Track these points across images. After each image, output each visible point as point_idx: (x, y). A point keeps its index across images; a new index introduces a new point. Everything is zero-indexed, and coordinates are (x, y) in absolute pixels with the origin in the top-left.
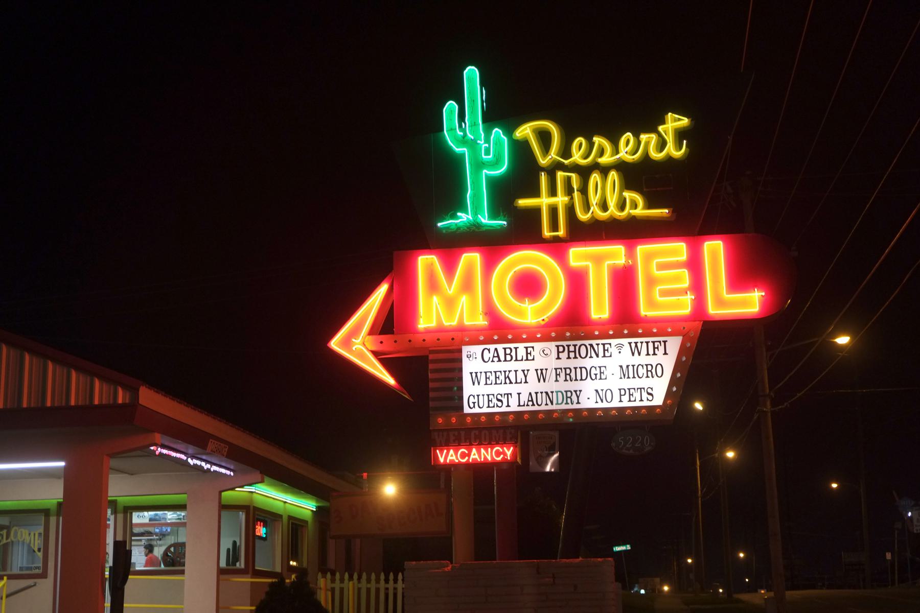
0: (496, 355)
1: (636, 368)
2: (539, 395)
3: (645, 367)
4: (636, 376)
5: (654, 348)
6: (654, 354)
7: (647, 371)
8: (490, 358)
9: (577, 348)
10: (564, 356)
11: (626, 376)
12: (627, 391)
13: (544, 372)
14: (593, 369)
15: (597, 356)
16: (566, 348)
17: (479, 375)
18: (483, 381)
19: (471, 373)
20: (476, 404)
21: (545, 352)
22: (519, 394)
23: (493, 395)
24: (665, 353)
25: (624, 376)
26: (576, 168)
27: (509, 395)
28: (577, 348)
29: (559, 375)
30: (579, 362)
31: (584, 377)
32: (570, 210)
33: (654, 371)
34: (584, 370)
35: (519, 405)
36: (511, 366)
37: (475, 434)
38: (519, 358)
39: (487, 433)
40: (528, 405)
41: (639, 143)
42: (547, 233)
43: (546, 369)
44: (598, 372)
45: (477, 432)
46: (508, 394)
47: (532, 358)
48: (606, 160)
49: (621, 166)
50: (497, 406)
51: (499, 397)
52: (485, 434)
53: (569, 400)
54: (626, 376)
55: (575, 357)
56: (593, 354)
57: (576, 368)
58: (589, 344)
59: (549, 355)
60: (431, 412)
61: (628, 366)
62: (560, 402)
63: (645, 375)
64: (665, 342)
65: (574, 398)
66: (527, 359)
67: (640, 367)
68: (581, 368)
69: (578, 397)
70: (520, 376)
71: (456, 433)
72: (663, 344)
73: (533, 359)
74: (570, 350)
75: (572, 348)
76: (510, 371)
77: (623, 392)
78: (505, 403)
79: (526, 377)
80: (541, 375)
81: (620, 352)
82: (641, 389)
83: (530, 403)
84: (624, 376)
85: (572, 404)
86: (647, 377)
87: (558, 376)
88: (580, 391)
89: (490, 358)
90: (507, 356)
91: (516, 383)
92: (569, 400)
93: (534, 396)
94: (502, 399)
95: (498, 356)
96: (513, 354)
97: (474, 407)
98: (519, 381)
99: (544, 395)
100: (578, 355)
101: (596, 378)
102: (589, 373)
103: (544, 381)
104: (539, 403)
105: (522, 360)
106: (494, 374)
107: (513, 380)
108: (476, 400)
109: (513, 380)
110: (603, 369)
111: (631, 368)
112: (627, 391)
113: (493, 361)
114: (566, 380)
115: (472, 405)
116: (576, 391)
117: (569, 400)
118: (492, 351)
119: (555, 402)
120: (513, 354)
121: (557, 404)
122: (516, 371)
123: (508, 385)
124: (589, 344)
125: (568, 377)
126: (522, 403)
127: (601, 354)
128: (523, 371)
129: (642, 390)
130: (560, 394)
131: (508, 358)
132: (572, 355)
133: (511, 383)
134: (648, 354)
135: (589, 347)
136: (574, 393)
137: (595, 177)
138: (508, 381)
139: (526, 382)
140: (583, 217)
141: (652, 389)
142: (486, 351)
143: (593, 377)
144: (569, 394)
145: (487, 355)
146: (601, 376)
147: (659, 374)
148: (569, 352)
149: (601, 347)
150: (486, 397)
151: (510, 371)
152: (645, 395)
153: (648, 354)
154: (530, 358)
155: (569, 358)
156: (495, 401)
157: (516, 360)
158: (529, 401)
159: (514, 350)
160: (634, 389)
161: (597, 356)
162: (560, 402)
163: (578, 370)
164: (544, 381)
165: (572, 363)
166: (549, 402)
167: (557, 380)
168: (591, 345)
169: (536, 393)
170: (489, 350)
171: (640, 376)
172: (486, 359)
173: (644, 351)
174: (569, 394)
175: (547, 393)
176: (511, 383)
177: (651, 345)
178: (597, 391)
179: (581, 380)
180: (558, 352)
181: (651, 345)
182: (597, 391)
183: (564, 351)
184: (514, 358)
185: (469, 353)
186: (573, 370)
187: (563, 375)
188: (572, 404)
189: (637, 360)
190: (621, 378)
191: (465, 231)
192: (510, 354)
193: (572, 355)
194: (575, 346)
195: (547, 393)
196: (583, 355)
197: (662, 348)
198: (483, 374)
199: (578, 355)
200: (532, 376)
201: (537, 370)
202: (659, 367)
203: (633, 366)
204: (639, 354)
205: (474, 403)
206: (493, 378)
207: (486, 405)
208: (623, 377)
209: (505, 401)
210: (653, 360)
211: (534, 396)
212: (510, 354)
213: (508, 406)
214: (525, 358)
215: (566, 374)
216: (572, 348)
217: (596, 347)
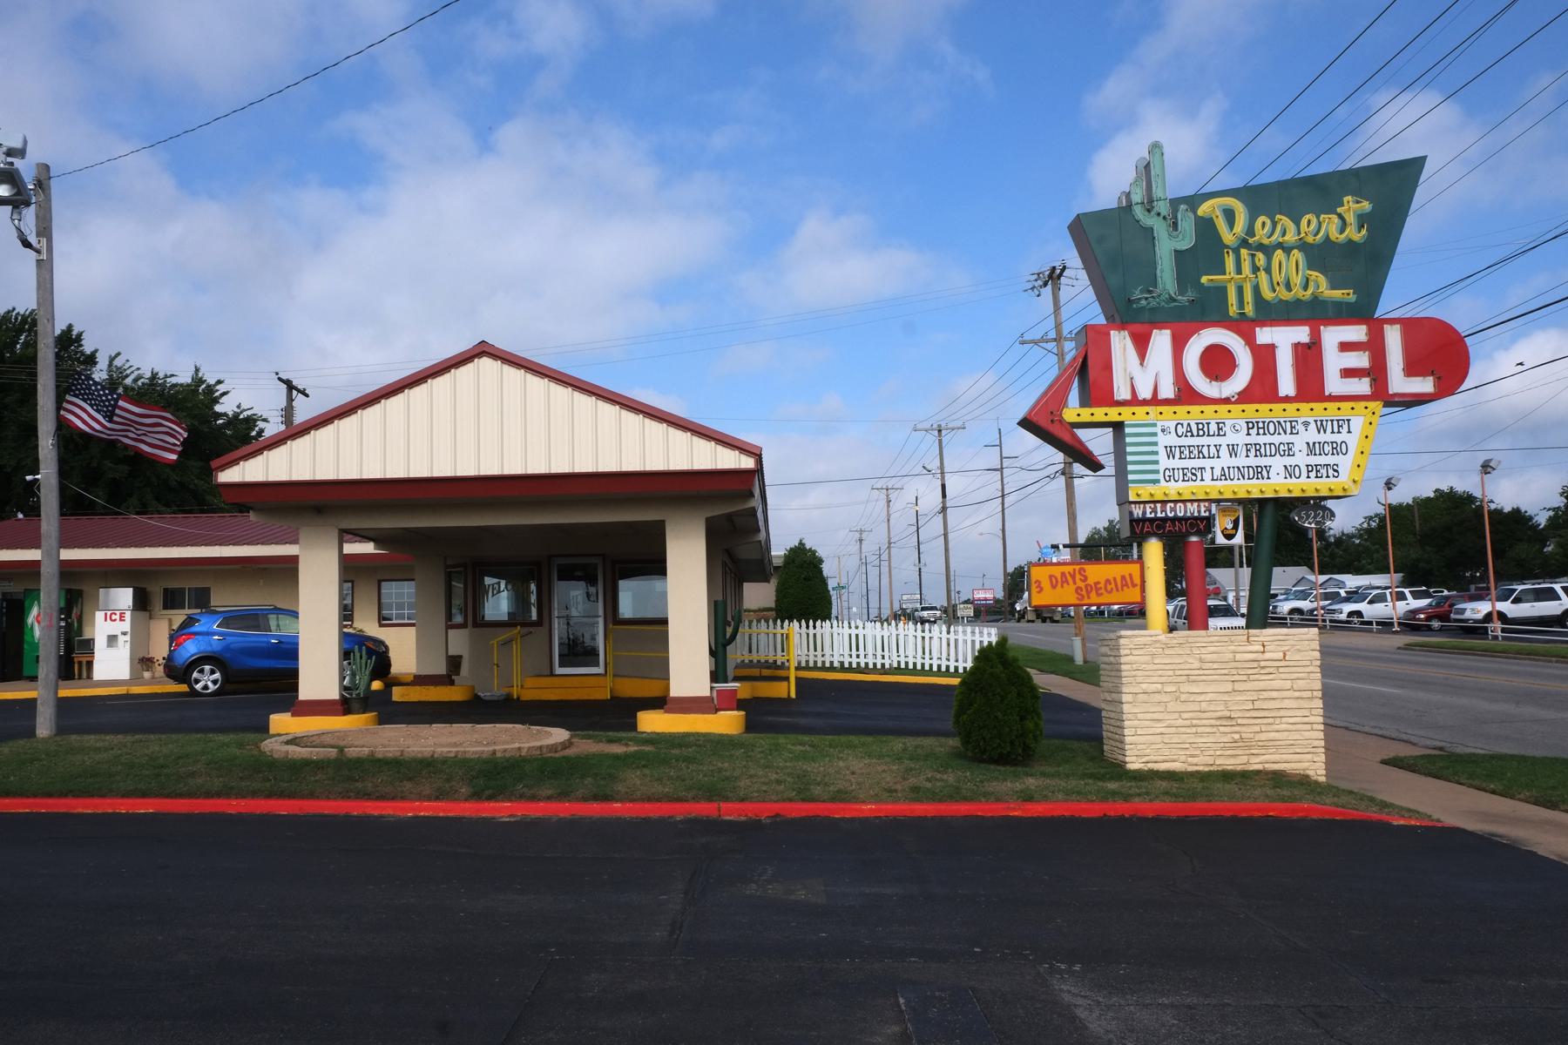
1: (1322, 444)
2: (1231, 470)
5: (1339, 426)
6: (1339, 432)
7: (1333, 448)
13: (1235, 447)
15: (1285, 433)
17: (1173, 449)
18: (1177, 455)
19: (1166, 447)
22: (1212, 468)
23: (1187, 469)
24: (1349, 432)
26: (1261, 247)
30: (1268, 439)
32: (1257, 290)
33: (1338, 448)
35: (1213, 480)
38: (1211, 433)
39: (1182, 505)
40: (1221, 480)
42: (1233, 310)
43: (1238, 445)
44: (1286, 448)
45: (1172, 505)
46: (1201, 469)
48: (1291, 237)
49: (1303, 246)
51: (1193, 471)
55: (1264, 434)
56: (1281, 431)
60: (1130, 485)
61: (1314, 443)
62: (1251, 477)
63: (1331, 452)
64: (1349, 420)
65: (1265, 473)
66: (1219, 435)
67: (1326, 444)
68: (1270, 444)
69: (1268, 472)
70: (1213, 450)
71: (1152, 506)
72: (1346, 422)
73: (1225, 435)
75: (1261, 425)
76: (1203, 446)
77: (1310, 468)
78: (1199, 478)
79: (1218, 451)
80: (1233, 451)
82: (1327, 465)
86: (1333, 454)
88: (1270, 467)
93: (1226, 470)
95: (1191, 431)
96: (1206, 429)
97: (1170, 480)
98: (1211, 456)
99: (1236, 469)
100: (1266, 432)
102: (1277, 450)
105: (1214, 435)
106: (1187, 448)
107: (1207, 456)
108: (1171, 474)
109: (1207, 456)
111: (1317, 445)
113: (1186, 436)
114: (1256, 456)
115: (1167, 479)
116: (1266, 467)
117: (1260, 475)
118: (1185, 425)
119: (1246, 477)
120: (1206, 429)
121: (1249, 479)
122: (1209, 446)
127: (1289, 431)
128: (1215, 446)
131: (1201, 433)
132: (1261, 431)
133: (1204, 457)
134: (1333, 432)
135: (1277, 424)
139: (1218, 457)
140: (1268, 294)
141: (1337, 465)
142: (1179, 426)
143: (1282, 453)
144: (1260, 470)
145: (1180, 432)
146: (1289, 452)
148: (1258, 428)
149: (1288, 424)
150: (1181, 471)
151: (1203, 446)
153: (1333, 432)
154: (1221, 433)
155: (1258, 434)
156: (1189, 474)
157: (1208, 435)
159: (1206, 426)
161: (1285, 433)
162: (1251, 477)
163: (1268, 446)
165: (1262, 439)
167: (1247, 456)
168: (1279, 422)
169: (1229, 468)
170: (1182, 425)
172: (1180, 434)
173: (1329, 429)
174: (1260, 470)
175: (1238, 468)
176: (1204, 457)
177: (1335, 423)
178: (1285, 466)
180: (1248, 429)
181: (1335, 423)
182: (1285, 466)
187: (1253, 450)
189: (1322, 437)
190: (1308, 455)
192: (1202, 429)
193: (1261, 431)
195: (1238, 468)
196: (1272, 431)
197: (1345, 427)
198: (1178, 449)
199: (1266, 432)
200: (1224, 452)
201: (1228, 445)
203: (1320, 443)
205: (1170, 476)
206: (1187, 452)
207: (1181, 478)
210: (1338, 438)
211: (1226, 470)
212: (1202, 429)
213: (1202, 480)
214: (1216, 433)
215: (1256, 450)
216: (1261, 425)
217: (1283, 424)
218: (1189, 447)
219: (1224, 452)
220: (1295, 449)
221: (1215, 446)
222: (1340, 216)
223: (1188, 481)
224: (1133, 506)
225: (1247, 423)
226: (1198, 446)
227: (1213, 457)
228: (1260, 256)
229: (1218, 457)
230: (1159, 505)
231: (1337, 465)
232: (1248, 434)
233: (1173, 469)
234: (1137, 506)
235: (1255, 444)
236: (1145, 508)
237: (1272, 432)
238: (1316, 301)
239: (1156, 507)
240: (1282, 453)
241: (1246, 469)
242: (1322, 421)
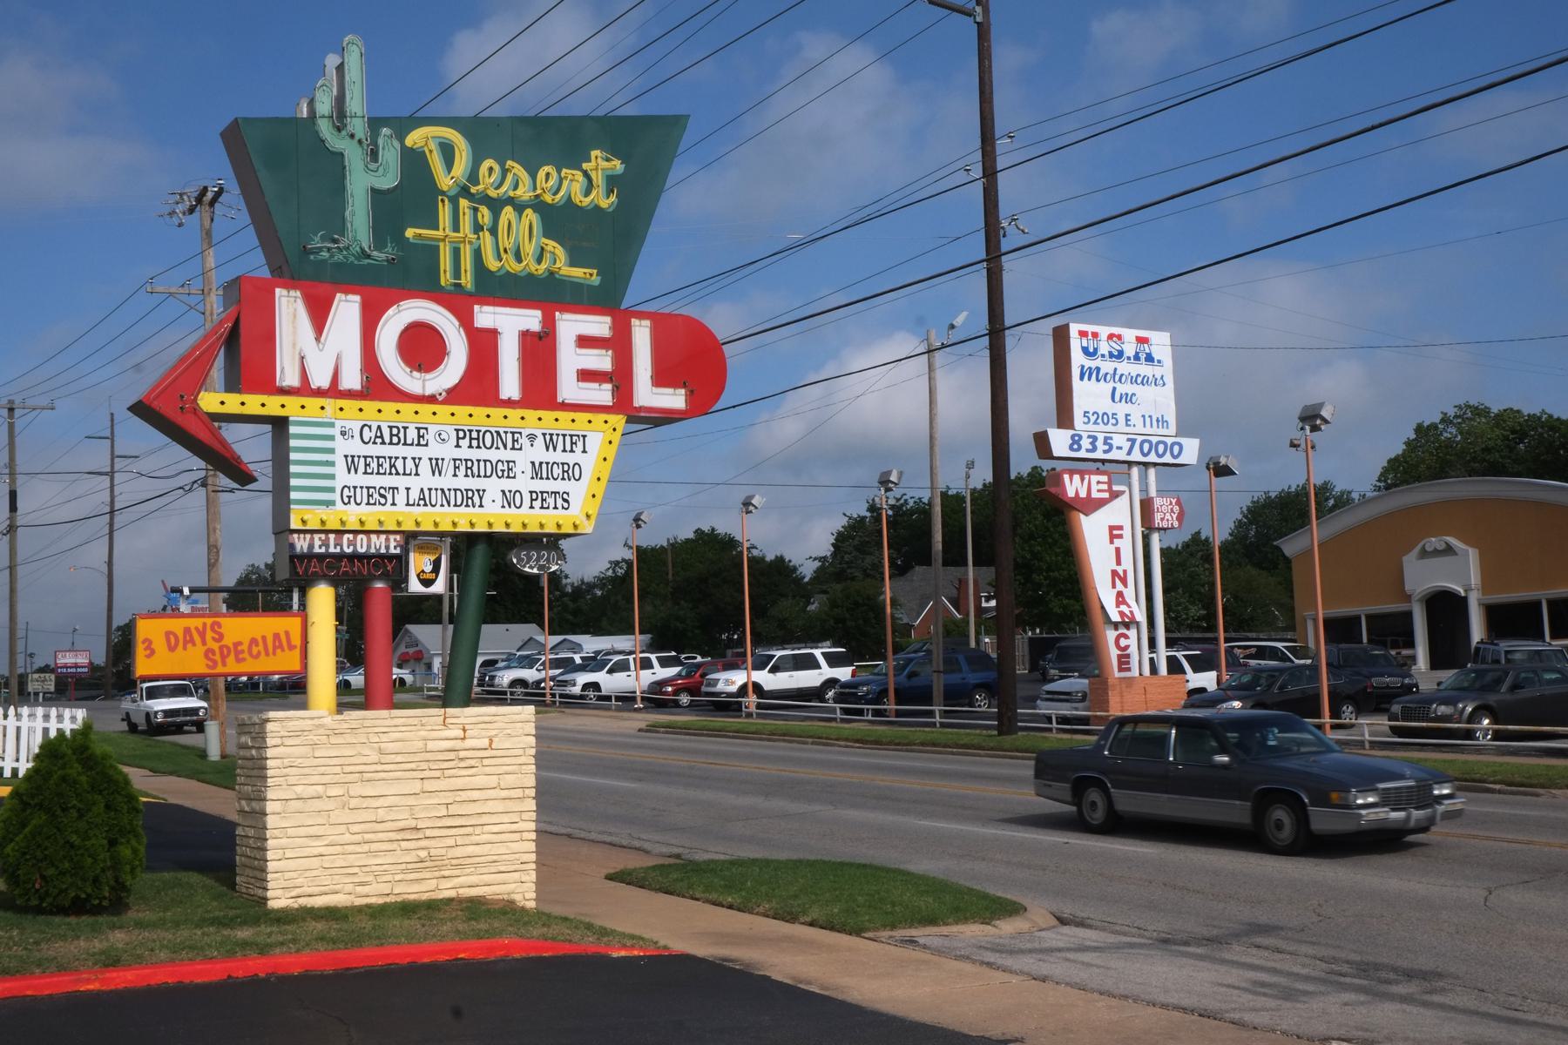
0: (379, 434)
1: (551, 465)
2: (433, 492)
3: (561, 466)
4: (550, 476)
5: (572, 443)
6: (572, 451)
7: (564, 471)
8: (371, 438)
9: (481, 434)
10: (465, 443)
11: (539, 476)
12: (540, 495)
13: (440, 462)
14: (500, 463)
16: (468, 433)
17: (356, 459)
19: (346, 456)
20: (352, 499)
21: (442, 437)
22: (408, 489)
23: (375, 488)
24: (584, 451)
25: (537, 475)
27: (396, 491)
28: (481, 434)
29: (458, 467)
30: (483, 454)
31: (488, 474)
32: (478, 255)
33: (570, 472)
34: (488, 464)
35: (408, 504)
36: (399, 451)
38: (409, 442)
40: (419, 505)
42: (446, 279)
43: (443, 459)
44: (506, 468)
45: (351, 536)
46: (393, 489)
47: (425, 443)
48: (524, 193)
49: (538, 205)
50: (380, 503)
51: (382, 491)
54: (539, 476)
55: (479, 447)
56: (500, 445)
57: (479, 461)
60: (292, 506)
61: (541, 463)
62: (459, 503)
63: (561, 476)
64: (584, 436)
65: (476, 499)
66: (419, 444)
67: (555, 466)
68: (485, 461)
69: (481, 498)
70: (410, 464)
71: (323, 536)
72: (581, 439)
73: (426, 445)
75: (474, 435)
76: (397, 458)
77: (534, 496)
78: (390, 501)
79: (417, 466)
80: (436, 466)
81: (532, 445)
82: (555, 493)
83: (422, 502)
84: (537, 475)
85: (474, 506)
86: (563, 479)
88: (484, 491)
89: (371, 438)
90: (476, 437)
91: (404, 474)
93: (427, 493)
94: (387, 494)
95: (382, 437)
96: (401, 435)
97: (349, 502)
98: (408, 472)
99: (440, 492)
100: (481, 445)
101: (503, 476)
102: (494, 469)
104: (433, 503)
105: (412, 444)
106: (375, 460)
107: (401, 471)
108: (352, 494)
109: (401, 471)
110: (511, 464)
111: (544, 466)
112: (540, 495)
113: (375, 443)
114: (466, 476)
115: (346, 500)
116: (478, 491)
117: (470, 501)
118: (374, 428)
119: (452, 503)
120: (401, 435)
121: (455, 505)
122: (404, 458)
126: (411, 502)
127: (509, 445)
128: (414, 459)
130: (459, 493)
132: (475, 443)
133: (397, 474)
134: (564, 451)
135: (495, 435)
136: (476, 493)
137: (508, 213)
138: (393, 471)
139: (417, 474)
140: (492, 264)
141: (568, 494)
142: (366, 429)
143: (500, 474)
144: (470, 494)
145: (367, 434)
146: (509, 472)
148: (471, 439)
149: (509, 436)
150: (365, 490)
151: (397, 458)
152: (560, 502)
153: (564, 451)
154: (422, 442)
155: (470, 446)
156: (376, 496)
157: (405, 444)
158: (420, 499)
159: (402, 430)
160: (548, 493)
162: (459, 503)
163: (482, 464)
165: (475, 454)
166: (445, 503)
167: (455, 475)
168: (498, 433)
169: (430, 490)
170: (370, 427)
171: (555, 476)
172: (366, 440)
173: (560, 447)
174: (470, 494)
175: (442, 490)
176: (397, 474)
177: (568, 438)
178: (503, 492)
179: (485, 476)
180: (458, 438)
181: (568, 438)
182: (503, 492)
183: (464, 438)
184: (402, 441)
185: (343, 429)
186: (476, 463)
187: (463, 468)
189: (551, 456)
190: (532, 478)
192: (397, 435)
193: (475, 443)
194: (478, 431)
195: (442, 490)
196: (488, 444)
197: (580, 444)
198: (362, 460)
199: (481, 445)
200: (425, 467)
201: (430, 459)
202: (577, 467)
203: (547, 463)
204: (555, 449)
205: (349, 497)
206: (374, 465)
207: (365, 501)
208: (534, 476)
210: (570, 458)
211: (427, 493)
212: (397, 435)
213: (394, 504)
214: (416, 442)
215: (467, 468)
216: (474, 435)
217: (503, 435)
218: (378, 458)
219: (425, 467)
220: (517, 470)
221: (414, 459)
222: (586, 174)
223: (375, 504)
224: (295, 536)
225: (457, 430)
226: (390, 458)
227: (410, 474)
228: (484, 210)
229: (417, 474)
230: (332, 536)
231: (568, 494)
232: (458, 446)
233: (355, 488)
234: (302, 536)
235: (466, 460)
236: (312, 539)
237: (488, 445)
239: (328, 539)
240: (500, 474)
241: (452, 493)
242: (551, 435)
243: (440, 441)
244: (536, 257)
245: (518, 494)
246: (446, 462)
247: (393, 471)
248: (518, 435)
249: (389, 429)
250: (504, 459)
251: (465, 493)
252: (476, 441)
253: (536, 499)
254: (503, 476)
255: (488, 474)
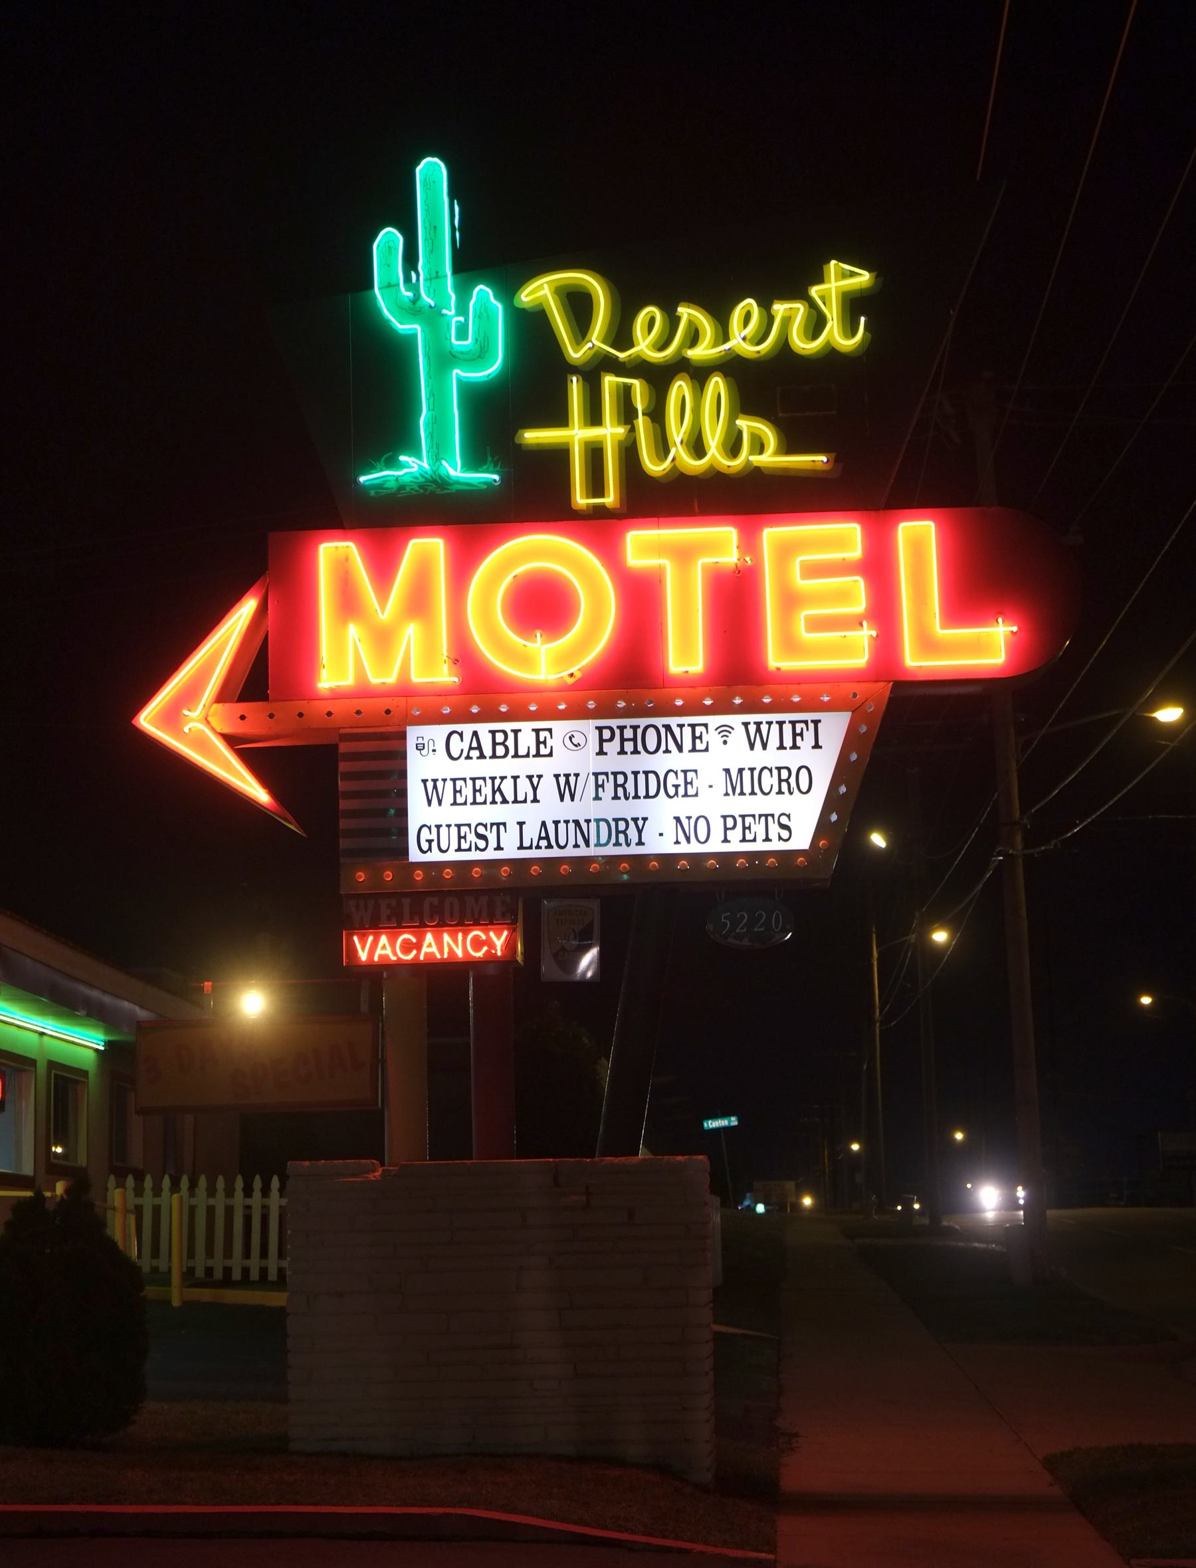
0: (475, 744)
1: (757, 774)
2: (562, 826)
3: (775, 772)
5: (795, 735)
6: (795, 746)
7: (780, 781)
8: (462, 751)
9: (640, 732)
10: (612, 747)
11: (738, 790)
12: (739, 820)
13: (572, 779)
14: (671, 775)
15: (680, 748)
16: (617, 732)
17: (440, 784)
18: (448, 797)
19: (425, 781)
20: (434, 844)
21: (575, 741)
22: (521, 824)
23: (469, 825)
24: (817, 746)
25: (734, 789)
26: (641, 369)
27: (502, 827)
28: (640, 732)
29: (602, 786)
30: (643, 762)
31: (652, 792)
32: (629, 452)
33: (793, 781)
34: (652, 777)
35: (521, 847)
36: (507, 767)
37: (431, 904)
38: (522, 752)
40: (538, 847)
41: (770, 320)
42: (581, 500)
43: (577, 775)
44: (681, 781)
45: (435, 901)
46: (498, 825)
47: (547, 752)
48: (702, 352)
49: (732, 367)
50: (477, 848)
51: (481, 830)
52: (452, 904)
53: (622, 837)
54: (738, 790)
55: (636, 752)
57: (636, 773)
58: (663, 726)
59: (582, 744)
60: (342, 860)
61: (741, 771)
63: (776, 789)
65: (632, 833)
66: (538, 755)
67: (766, 772)
68: (646, 773)
69: (640, 832)
70: (524, 787)
71: (393, 903)
72: (811, 726)
74: (626, 736)
75: (628, 733)
76: (503, 778)
77: (730, 822)
78: (493, 843)
79: (535, 789)
80: (566, 787)
81: (725, 742)
82: (766, 816)
83: (544, 843)
84: (734, 789)
85: (628, 845)
86: (780, 792)
87: (600, 789)
88: (645, 819)
89: (462, 751)
90: (497, 747)
91: (516, 801)
92: (622, 837)
94: (487, 834)
95: (479, 748)
96: (510, 743)
97: (430, 849)
98: (521, 797)
99: (572, 826)
100: (640, 748)
101: (676, 794)
102: (662, 784)
103: (572, 798)
104: (562, 843)
105: (527, 755)
106: (470, 783)
107: (510, 797)
108: (434, 836)
109: (510, 797)
110: (690, 775)
112: (739, 820)
113: (468, 757)
114: (616, 797)
115: (425, 846)
116: (635, 820)
117: (621, 837)
118: (467, 736)
119: (593, 841)
120: (510, 743)
121: (598, 844)
122: (515, 778)
123: (499, 807)
124: (663, 726)
125: (620, 791)
126: (526, 843)
127: (687, 745)
128: (530, 777)
129: (770, 818)
130: (603, 825)
131: (500, 750)
132: (629, 746)
133: (505, 801)
134: (781, 747)
135: (663, 731)
136: (632, 824)
137: (680, 388)
138: (498, 798)
139: (535, 800)
140: (654, 467)
141: (789, 816)
142: (455, 737)
143: (672, 791)
144: (622, 826)
145: (456, 746)
146: (687, 789)
147: (804, 787)
148: (623, 740)
149: (687, 731)
150: (454, 830)
151: (503, 778)
152: (774, 830)
153: (781, 747)
154: (543, 751)
155: (622, 752)
156: (471, 837)
157: (516, 755)
158: (540, 838)
159: (511, 736)
160: (754, 816)
161: (680, 748)
163: (641, 777)
164: (572, 798)
165: (629, 763)
166: (581, 841)
167: (597, 798)
168: (668, 728)
169: (556, 823)
170: (461, 735)
171: (766, 790)
172: (455, 754)
174: (622, 826)
175: (577, 823)
176: (505, 801)
177: (787, 728)
178: (678, 819)
179: (647, 796)
182: (678, 819)
184: (512, 752)
185: (420, 741)
186: (631, 778)
187: (610, 787)
188: (628, 845)
189: (759, 758)
190: (727, 794)
191: (415, 493)
192: (503, 744)
193: (629, 746)
194: (635, 728)
195: (577, 823)
196: (652, 746)
197: (809, 736)
198: (449, 784)
199: (640, 748)
200: (548, 789)
201: (557, 776)
202: (804, 772)
203: (752, 770)
204: (764, 746)
205: (430, 842)
206: (468, 791)
207: (454, 845)
208: (730, 791)
209: (492, 838)
210: (791, 759)
212: (503, 744)
213: (499, 848)
214: (533, 751)
215: (616, 786)
216: (628, 733)
217: (677, 731)
218: (474, 780)
219: (548, 789)
220: (699, 783)
221: (530, 777)
222: (812, 304)
223: (469, 849)
226: (493, 779)
227: (525, 801)
228: (637, 386)
229: (535, 800)
231: (789, 816)
233: (438, 827)
235: (615, 774)
237: (652, 747)
238: (755, 475)
240: (672, 791)
241: (593, 825)
242: (758, 724)
243: (575, 748)
244: (730, 446)
245: (702, 821)
246: (581, 780)
247: (498, 798)
248: (703, 729)
249: (490, 735)
250: (679, 768)
251: (613, 824)
252: (631, 743)
253: (734, 827)
254: (676, 794)
255: (652, 792)
